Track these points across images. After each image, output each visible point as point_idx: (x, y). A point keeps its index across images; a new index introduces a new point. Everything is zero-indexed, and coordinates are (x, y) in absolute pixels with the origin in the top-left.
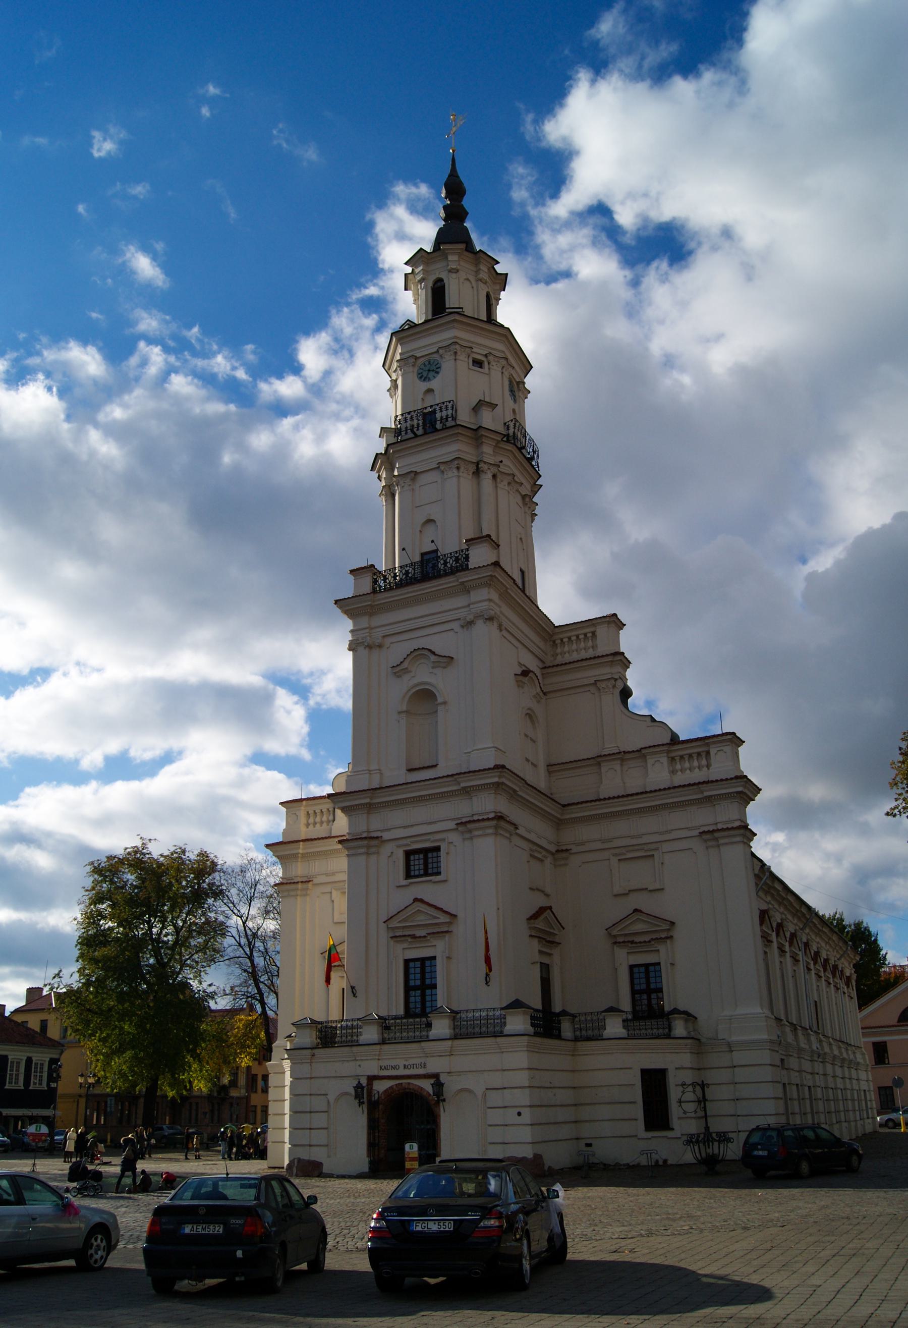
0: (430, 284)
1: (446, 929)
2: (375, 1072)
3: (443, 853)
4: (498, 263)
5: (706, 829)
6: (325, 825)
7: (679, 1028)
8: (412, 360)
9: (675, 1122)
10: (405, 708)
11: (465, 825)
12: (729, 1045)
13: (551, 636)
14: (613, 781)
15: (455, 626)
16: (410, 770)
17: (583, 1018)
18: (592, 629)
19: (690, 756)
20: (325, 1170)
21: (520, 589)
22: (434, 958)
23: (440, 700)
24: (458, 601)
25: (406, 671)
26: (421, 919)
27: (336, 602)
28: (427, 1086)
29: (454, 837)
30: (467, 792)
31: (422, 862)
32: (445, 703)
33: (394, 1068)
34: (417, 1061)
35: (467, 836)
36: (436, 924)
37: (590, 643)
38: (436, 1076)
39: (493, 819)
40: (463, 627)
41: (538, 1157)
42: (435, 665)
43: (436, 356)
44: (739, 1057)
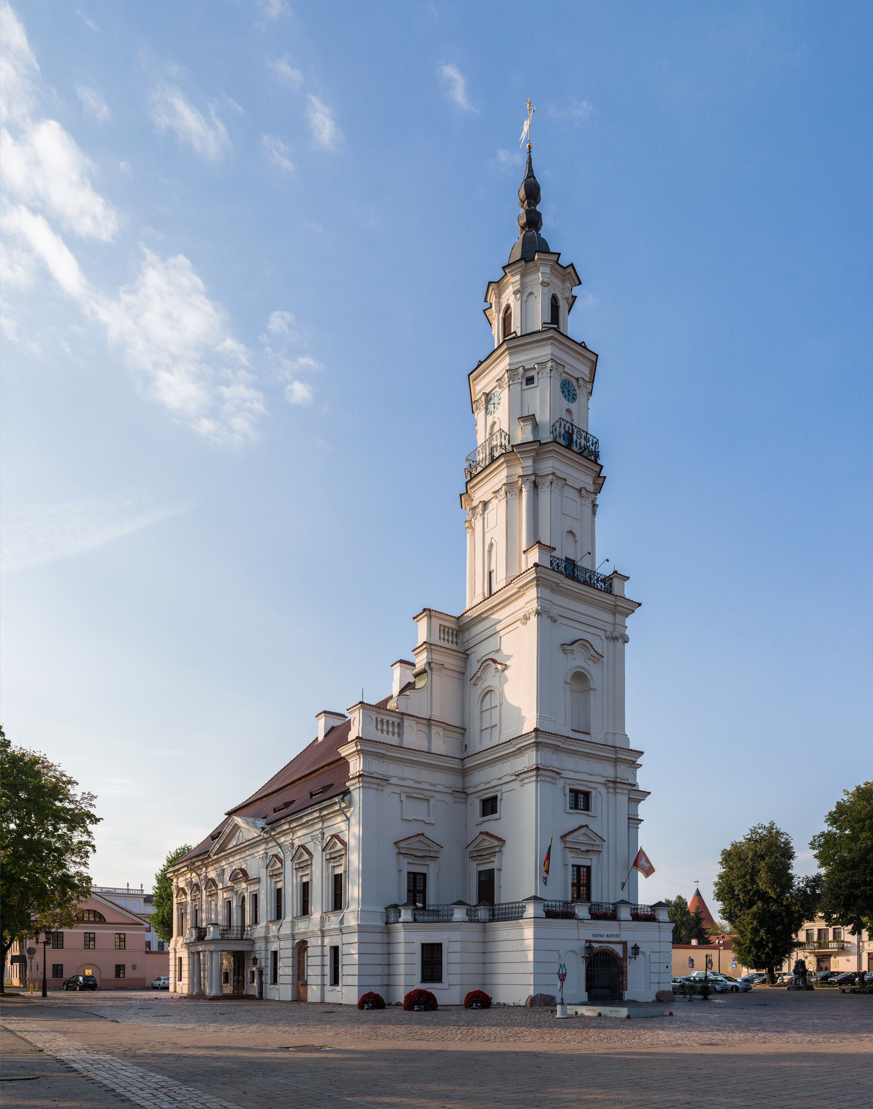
6: (396, 736)
15: (602, 634)
24: (608, 617)
28: (618, 949)
31: (580, 800)
33: (601, 936)
34: (615, 933)
36: (593, 845)
38: (624, 944)
40: (607, 638)
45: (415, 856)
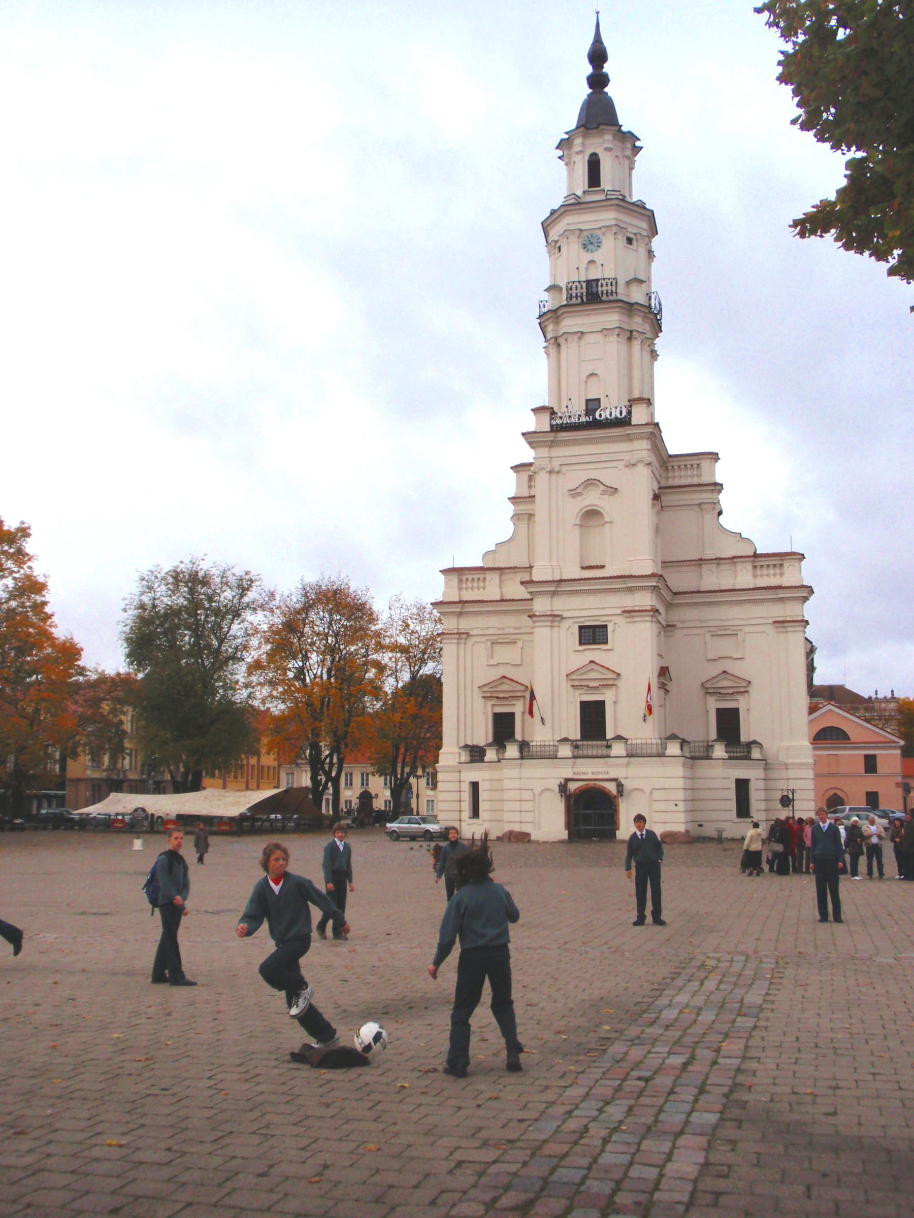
0: (587, 158)
1: (611, 683)
2: (570, 776)
3: (610, 629)
4: (639, 140)
5: (777, 619)
7: (756, 754)
8: (578, 233)
9: (753, 812)
10: (578, 522)
11: (629, 613)
12: (786, 764)
13: (665, 463)
14: (712, 579)
15: (620, 465)
16: (583, 568)
17: (696, 744)
18: (698, 462)
19: (768, 566)
20: (534, 837)
21: (654, 432)
23: (607, 519)
25: (580, 494)
26: (593, 675)
27: (523, 434)
29: (621, 620)
30: (631, 590)
31: (593, 634)
32: (611, 522)
33: (584, 774)
35: (629, 620)
37: (695, 473)
38: (615, 780)
39: (649, 611)
40: (626, 466)
41: (687, 831)
42: (604, 493)
43: (599, 233)
44: (792, 773)
45: (497, 698)
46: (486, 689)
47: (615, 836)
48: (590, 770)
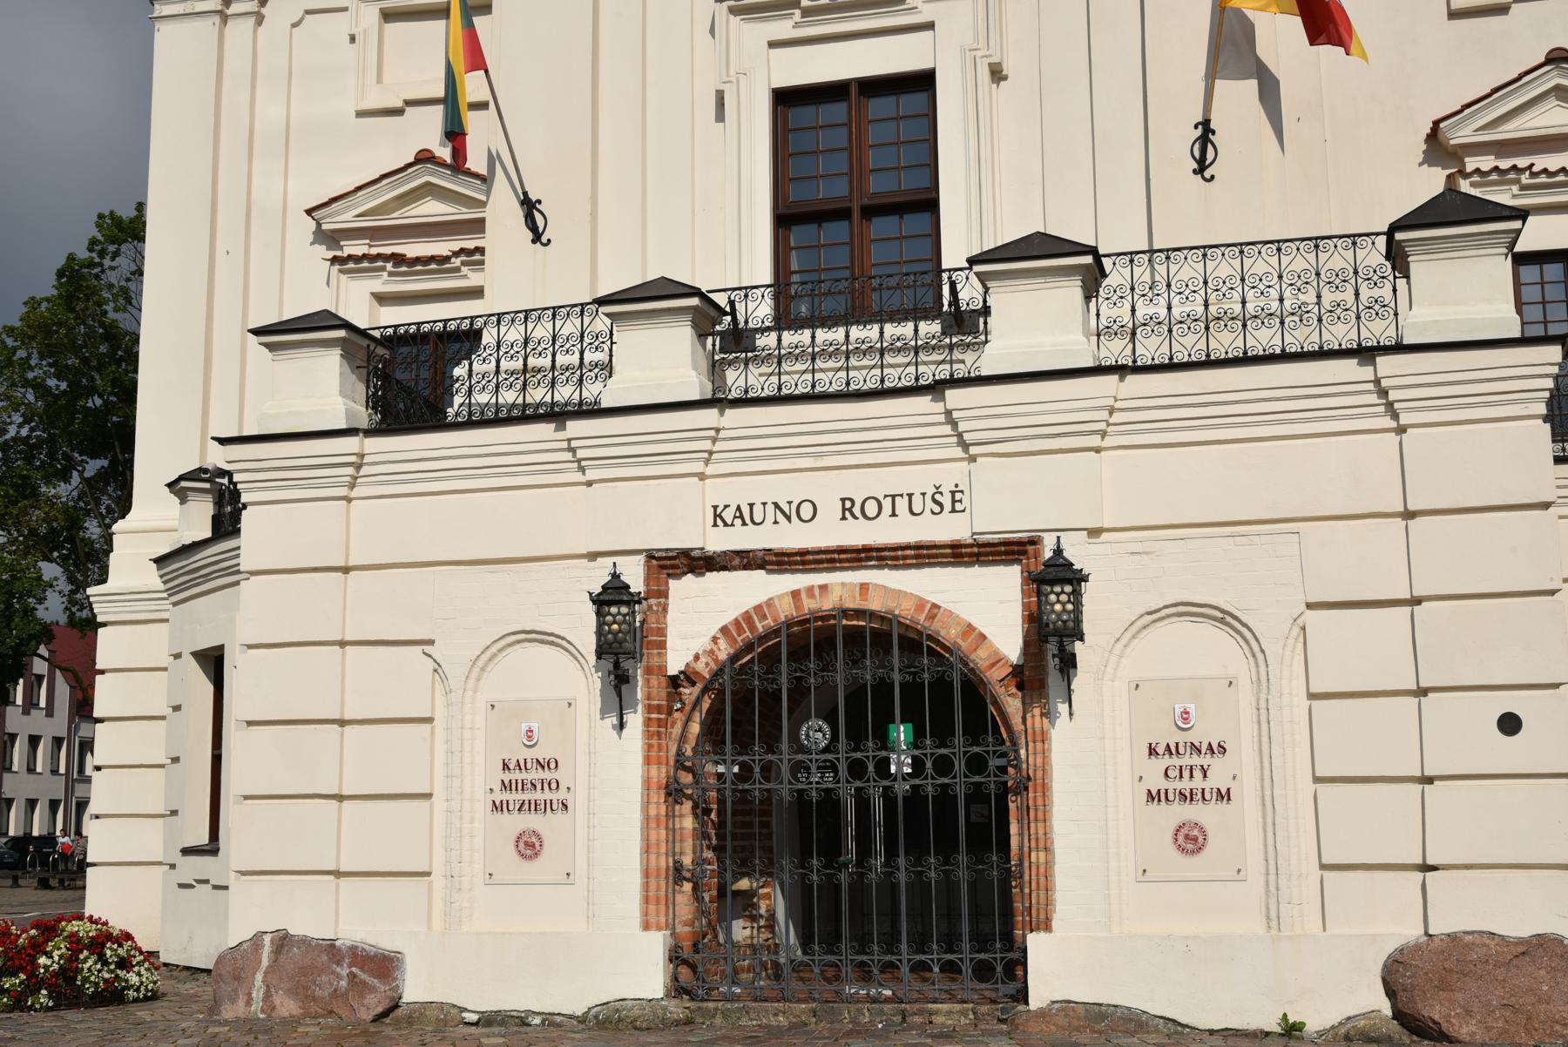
22: (923, 82)
34: (919, 480)
45: (398, 259)
46: (344, 218)
47: (1011, 970)
48: (827, 491)
